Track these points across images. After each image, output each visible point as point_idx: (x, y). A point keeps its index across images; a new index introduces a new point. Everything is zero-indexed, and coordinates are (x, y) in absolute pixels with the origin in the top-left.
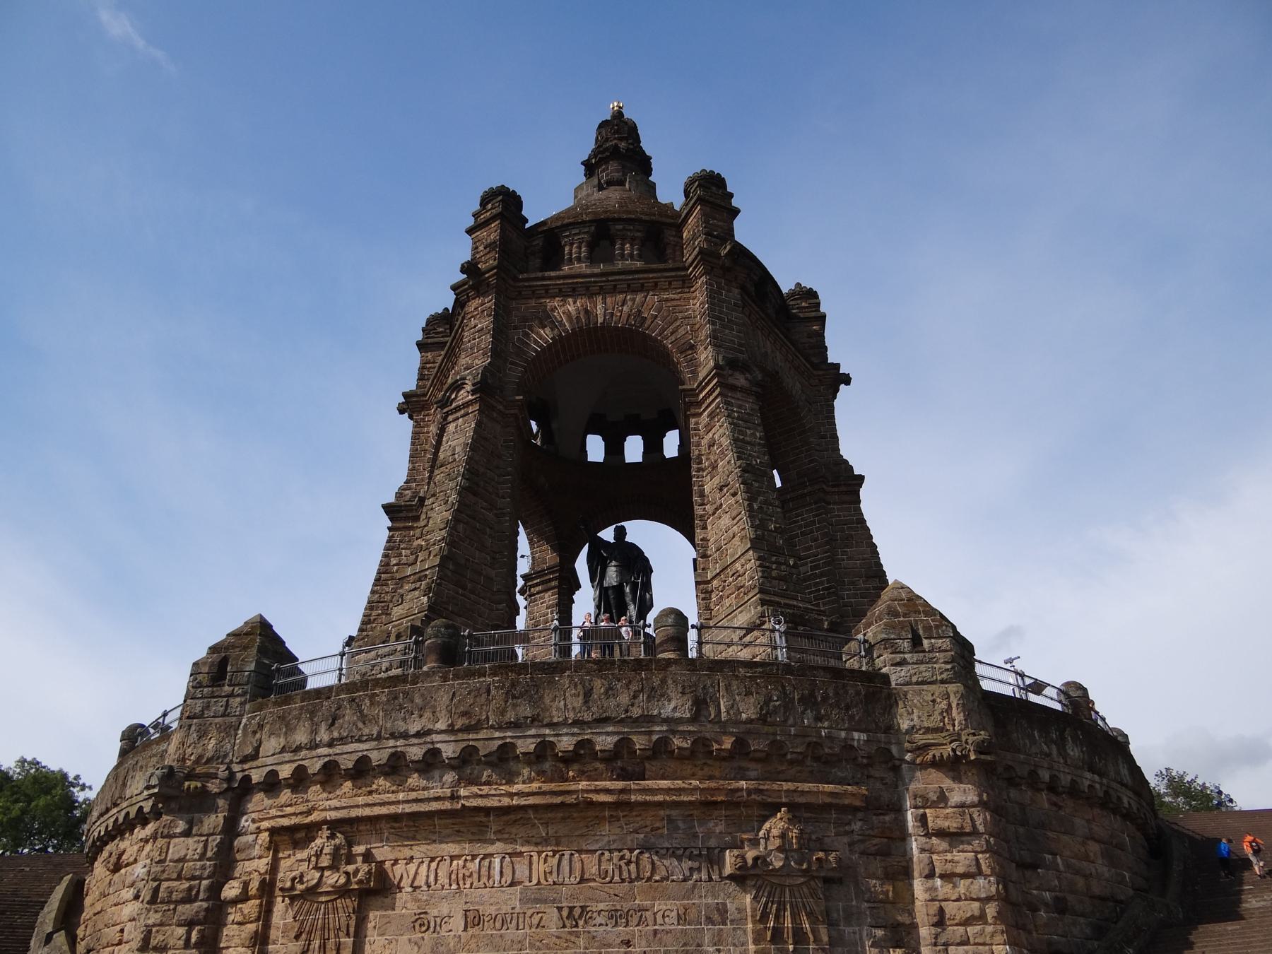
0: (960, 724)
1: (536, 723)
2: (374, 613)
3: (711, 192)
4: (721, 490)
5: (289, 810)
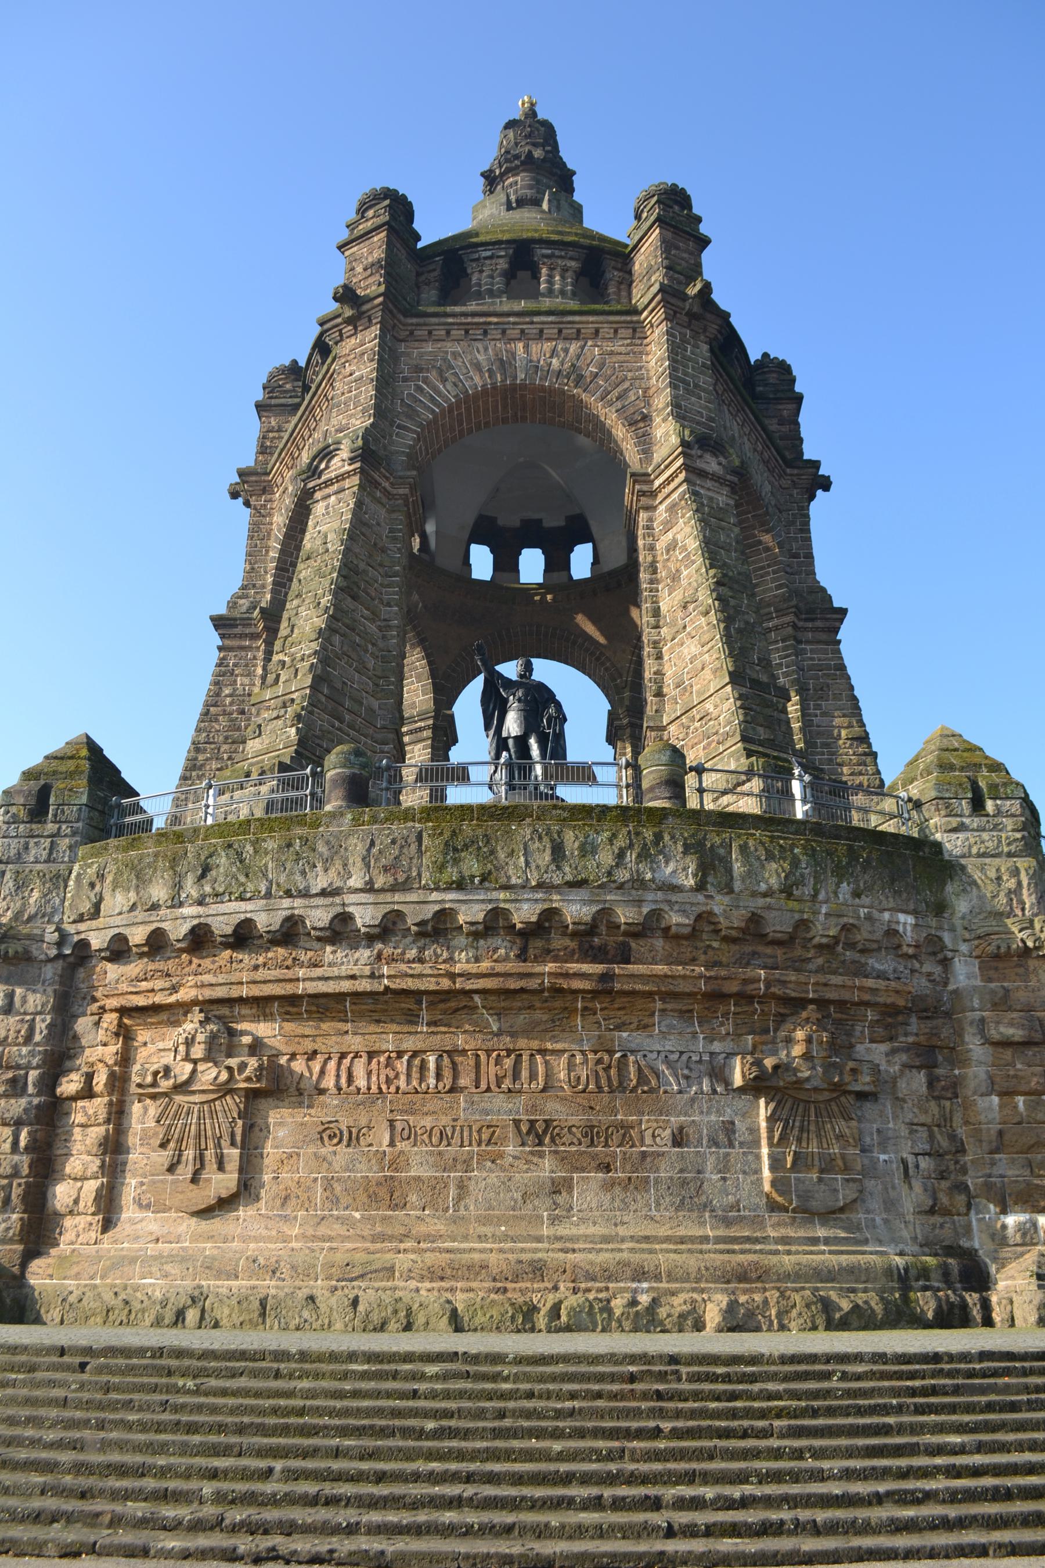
0: (1031, 908)
1: (487, 884)
2: (201, 757)
3: (675, 214)
4: (685, 607)
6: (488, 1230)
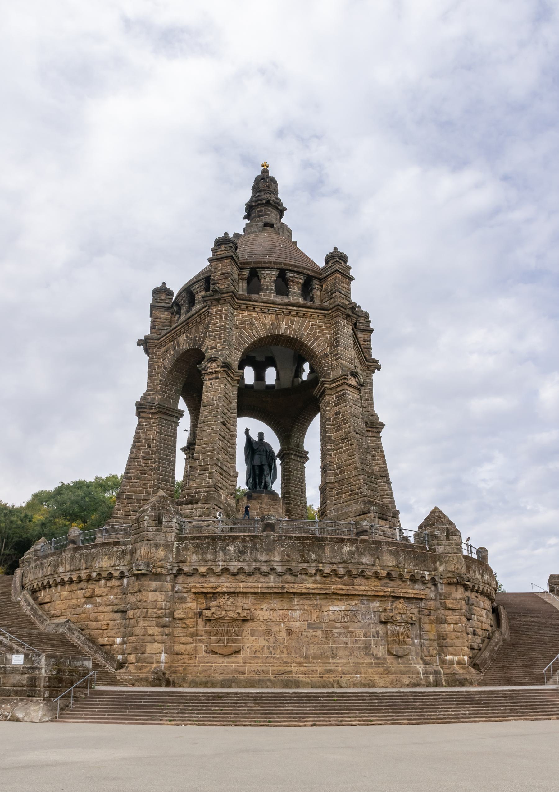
5: (205, 585)
6: (315, 661)
